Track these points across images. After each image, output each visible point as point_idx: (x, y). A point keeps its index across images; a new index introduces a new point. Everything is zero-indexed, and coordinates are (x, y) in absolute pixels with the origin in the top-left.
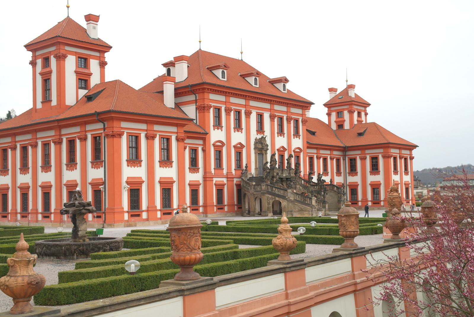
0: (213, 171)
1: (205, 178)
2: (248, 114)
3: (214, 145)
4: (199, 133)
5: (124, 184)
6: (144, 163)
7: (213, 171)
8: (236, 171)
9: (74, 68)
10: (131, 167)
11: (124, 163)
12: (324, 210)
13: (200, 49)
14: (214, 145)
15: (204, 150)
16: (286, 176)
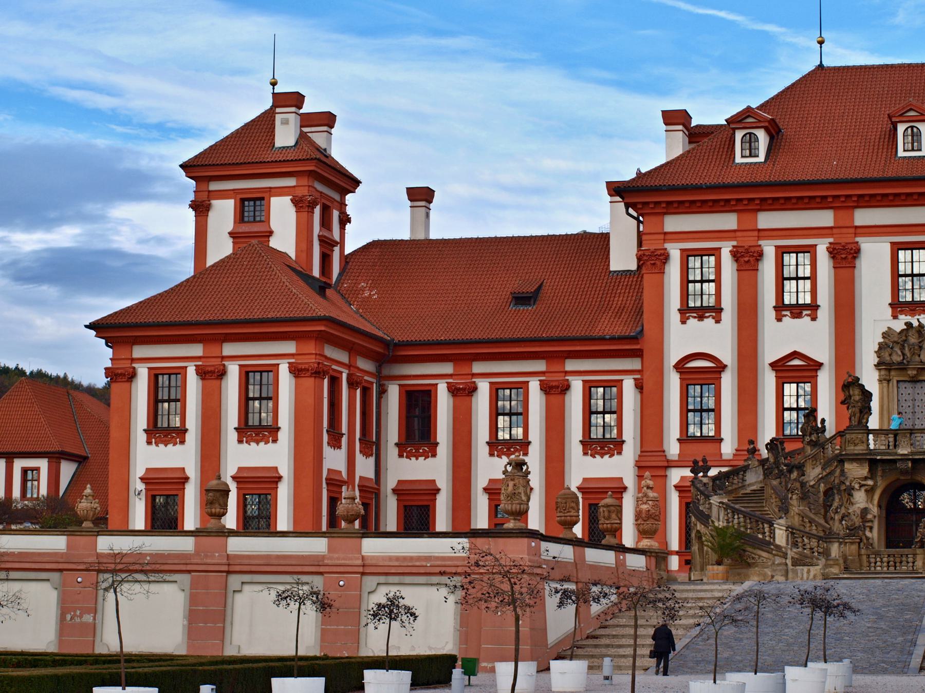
0: (673, 449)
1: (640, 467)
2: (845, 257)
3: (680, 366)
4: (602, 339)
5: (140, 486)
6: (192, 437)
7: (673, 449)
8: (683, 445)
9: (230, 226)
10: (157, 445)
11: (139, 437)
12: (822, 561)
13: (821, 66)
14: (680, 366)
15: (639, 386)
16: (912, 453)
